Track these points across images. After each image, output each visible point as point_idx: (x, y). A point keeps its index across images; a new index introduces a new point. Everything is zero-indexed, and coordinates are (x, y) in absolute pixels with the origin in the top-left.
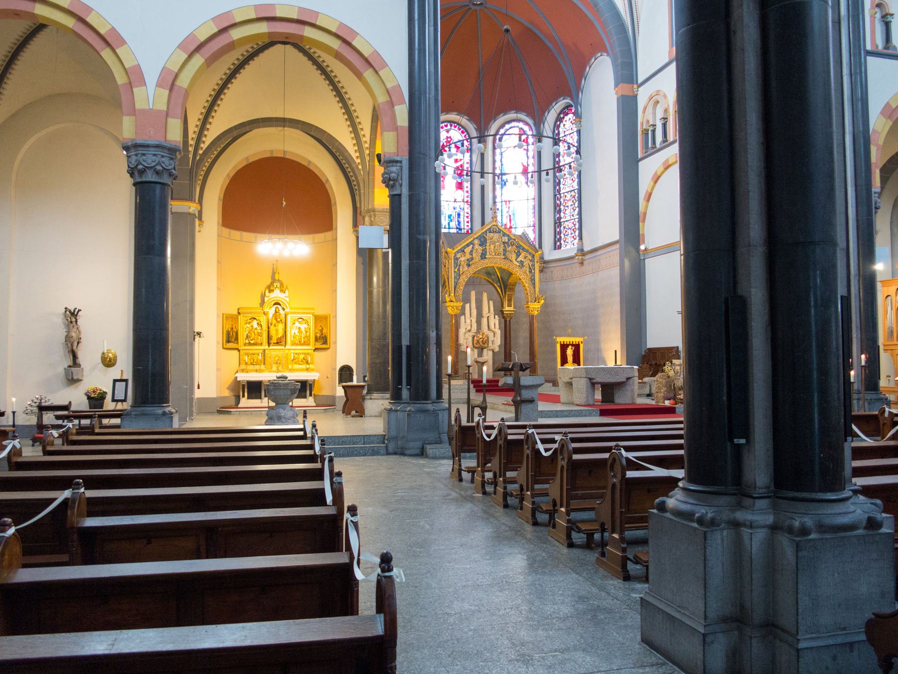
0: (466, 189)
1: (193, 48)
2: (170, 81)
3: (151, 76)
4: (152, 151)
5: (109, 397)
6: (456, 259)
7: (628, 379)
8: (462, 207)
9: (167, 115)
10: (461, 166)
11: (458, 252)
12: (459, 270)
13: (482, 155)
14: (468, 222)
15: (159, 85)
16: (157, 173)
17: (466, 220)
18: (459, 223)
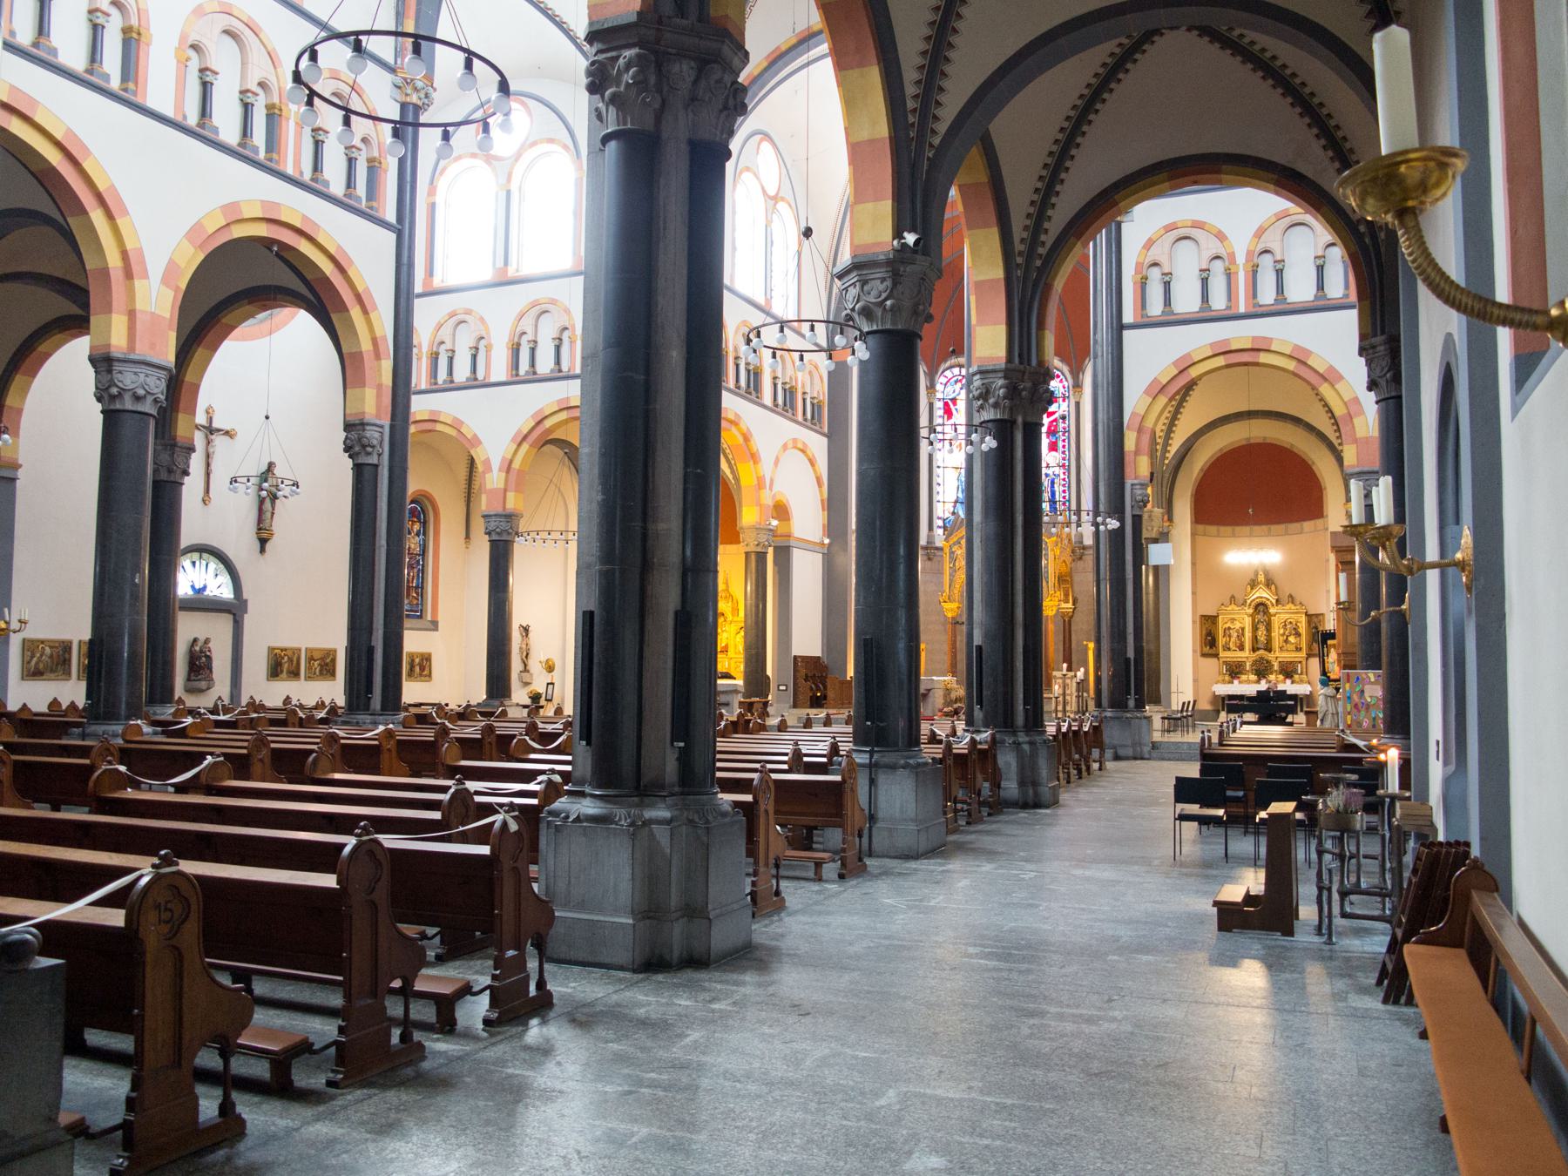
0: (1061, 449)
1: (519, 439)
2: (508, 467)
3: (496, 464)
4: (494, 519)
5: (544, 696)
6: (952, 553)
7: (929, 690)
8: (1057, 473)
9: (505, 490)
10: (1055, 420)
11: (954, 544)
12: (954, 565)
13: (1078, 404)
14: (1064, 491)
15: (500, 470)
16: (498, 533)
17: (1062, 488)
18: (1053, 494)
